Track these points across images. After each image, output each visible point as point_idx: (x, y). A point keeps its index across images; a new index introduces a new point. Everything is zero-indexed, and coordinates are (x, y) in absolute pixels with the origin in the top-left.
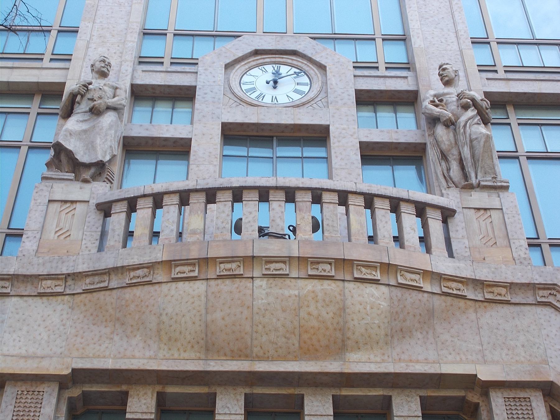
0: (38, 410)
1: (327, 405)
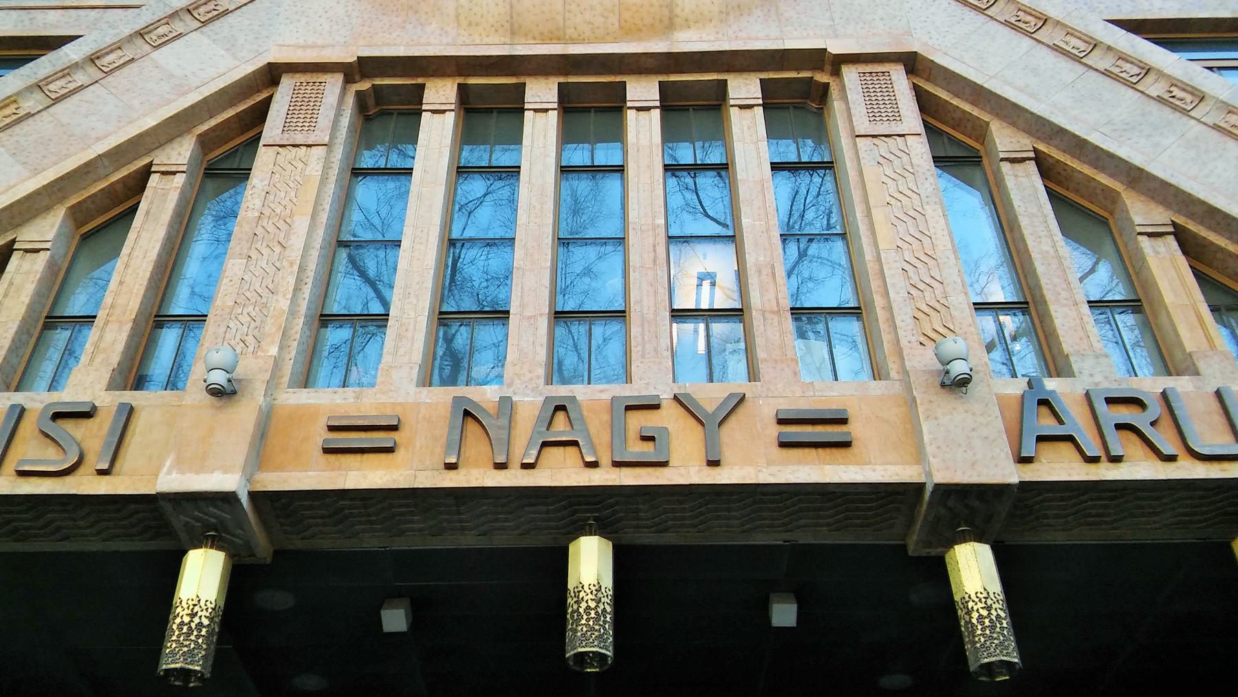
0: (319, 100)
1: (652, 91)
